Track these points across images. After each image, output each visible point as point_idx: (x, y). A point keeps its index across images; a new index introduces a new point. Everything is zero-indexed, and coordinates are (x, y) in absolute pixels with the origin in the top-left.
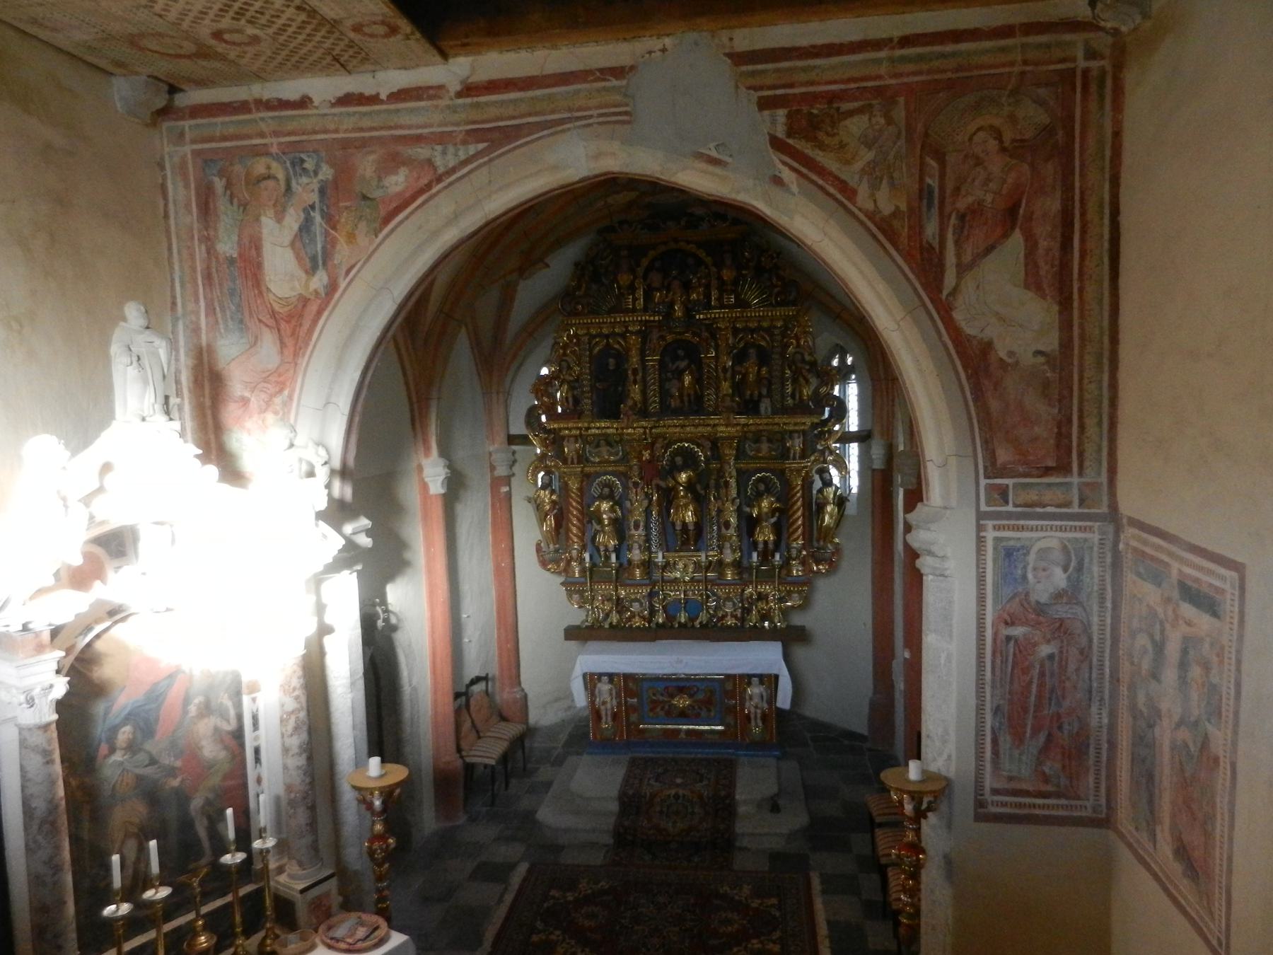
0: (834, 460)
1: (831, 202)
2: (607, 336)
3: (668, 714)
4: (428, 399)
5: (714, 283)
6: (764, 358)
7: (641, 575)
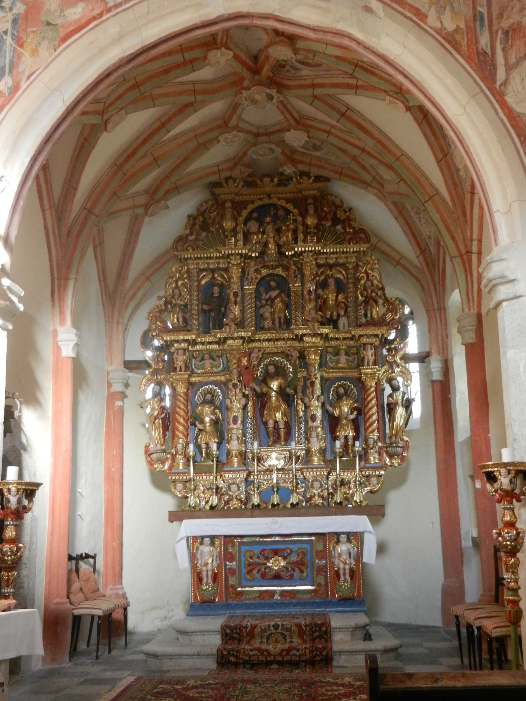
0: (401, 372)
1: (408, 22)
2: (213, 271)
3: (263, 576)
4: (67, 279)
5: (301, 228)
6: (340, 287)
7: (238, 463)
